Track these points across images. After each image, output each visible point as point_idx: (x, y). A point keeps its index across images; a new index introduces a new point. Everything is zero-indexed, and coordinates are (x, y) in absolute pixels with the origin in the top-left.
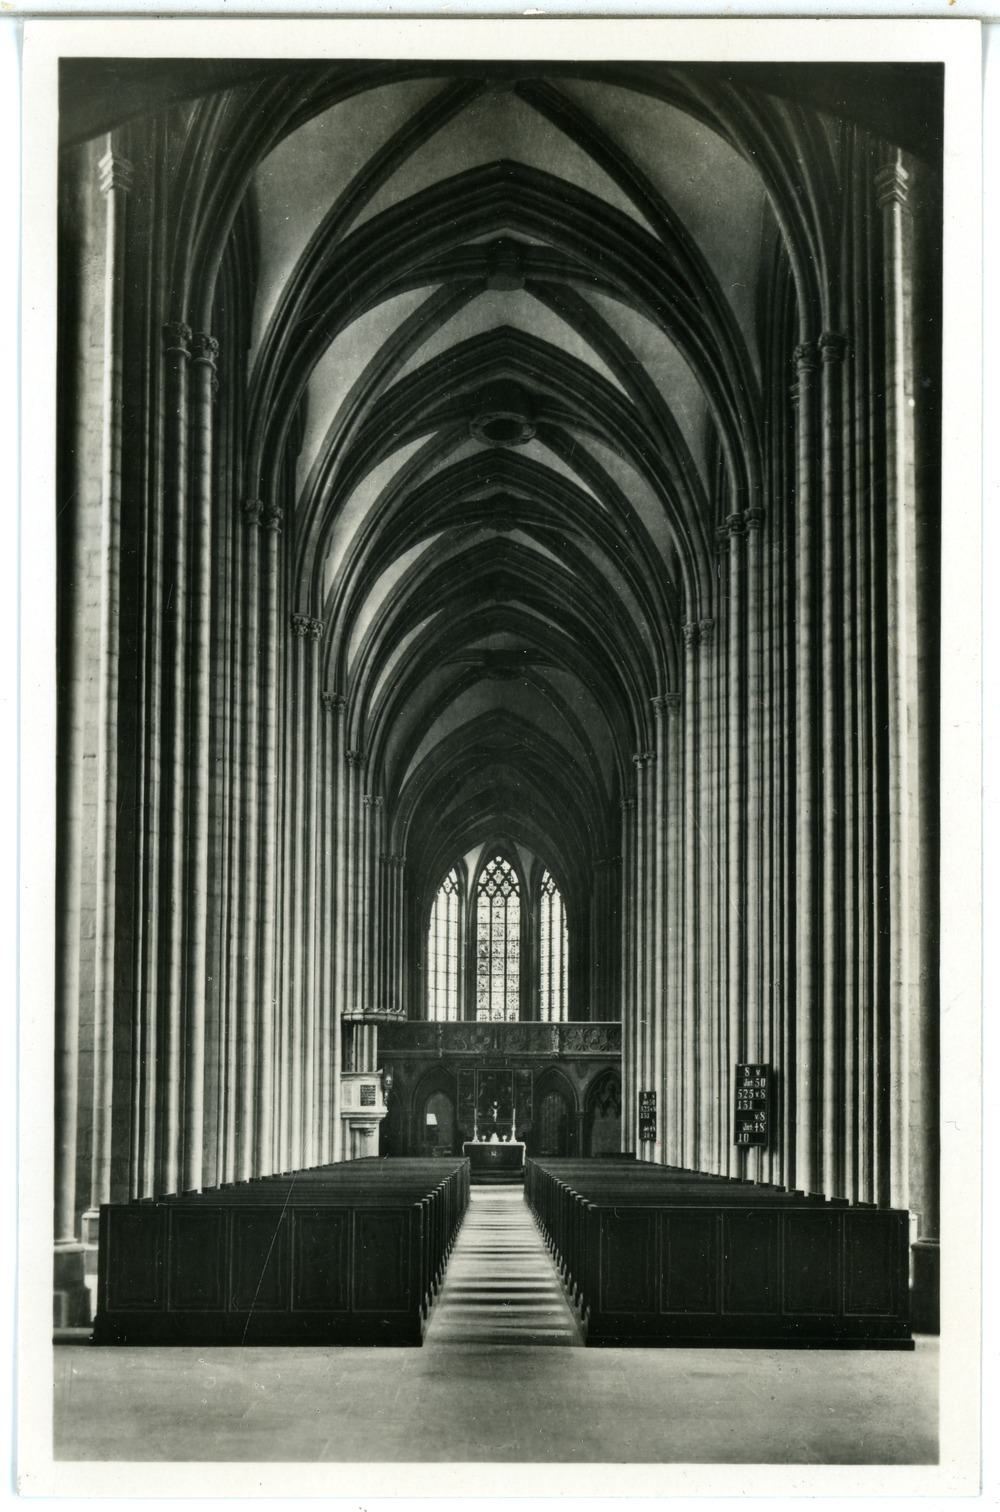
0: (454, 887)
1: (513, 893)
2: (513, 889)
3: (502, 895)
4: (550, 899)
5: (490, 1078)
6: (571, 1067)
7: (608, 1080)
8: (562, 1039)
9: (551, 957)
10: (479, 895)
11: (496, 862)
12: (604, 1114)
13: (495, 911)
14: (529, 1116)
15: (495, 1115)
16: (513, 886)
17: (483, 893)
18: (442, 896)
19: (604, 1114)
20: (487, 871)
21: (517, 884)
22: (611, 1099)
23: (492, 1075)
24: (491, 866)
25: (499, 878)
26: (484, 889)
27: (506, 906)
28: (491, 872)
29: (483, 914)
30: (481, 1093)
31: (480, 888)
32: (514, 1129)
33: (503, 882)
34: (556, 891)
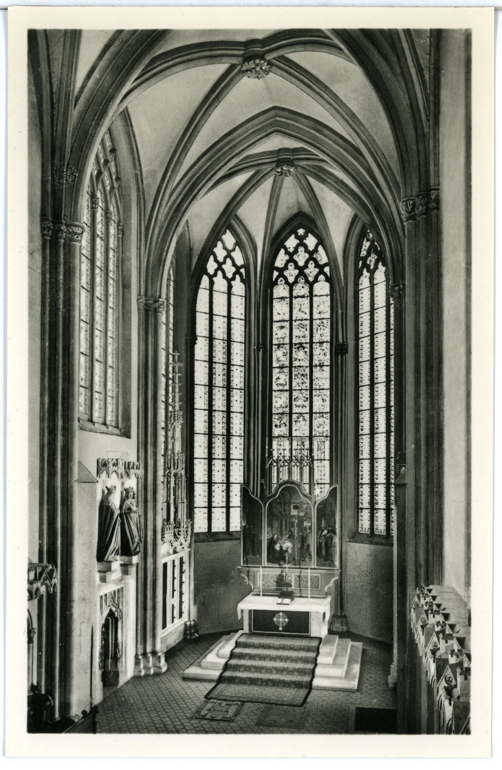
0: (238, 272)
1: (322, 277)
2: (321, 272)
3: (307, 281)
4: (372, 279)
9: (372, 360)
10: (276, 283)
11: (297, 237)
16: (321, 268)
18: (220, 284)
20: (286, 249)
21: (326, 265)
24: (291, 243)
25: (301, 258)
26: (281, 275)
27: (311, 295)
28: (291, 250)
29: (280, 310)
31: (276, 274)
34: (380, 265)
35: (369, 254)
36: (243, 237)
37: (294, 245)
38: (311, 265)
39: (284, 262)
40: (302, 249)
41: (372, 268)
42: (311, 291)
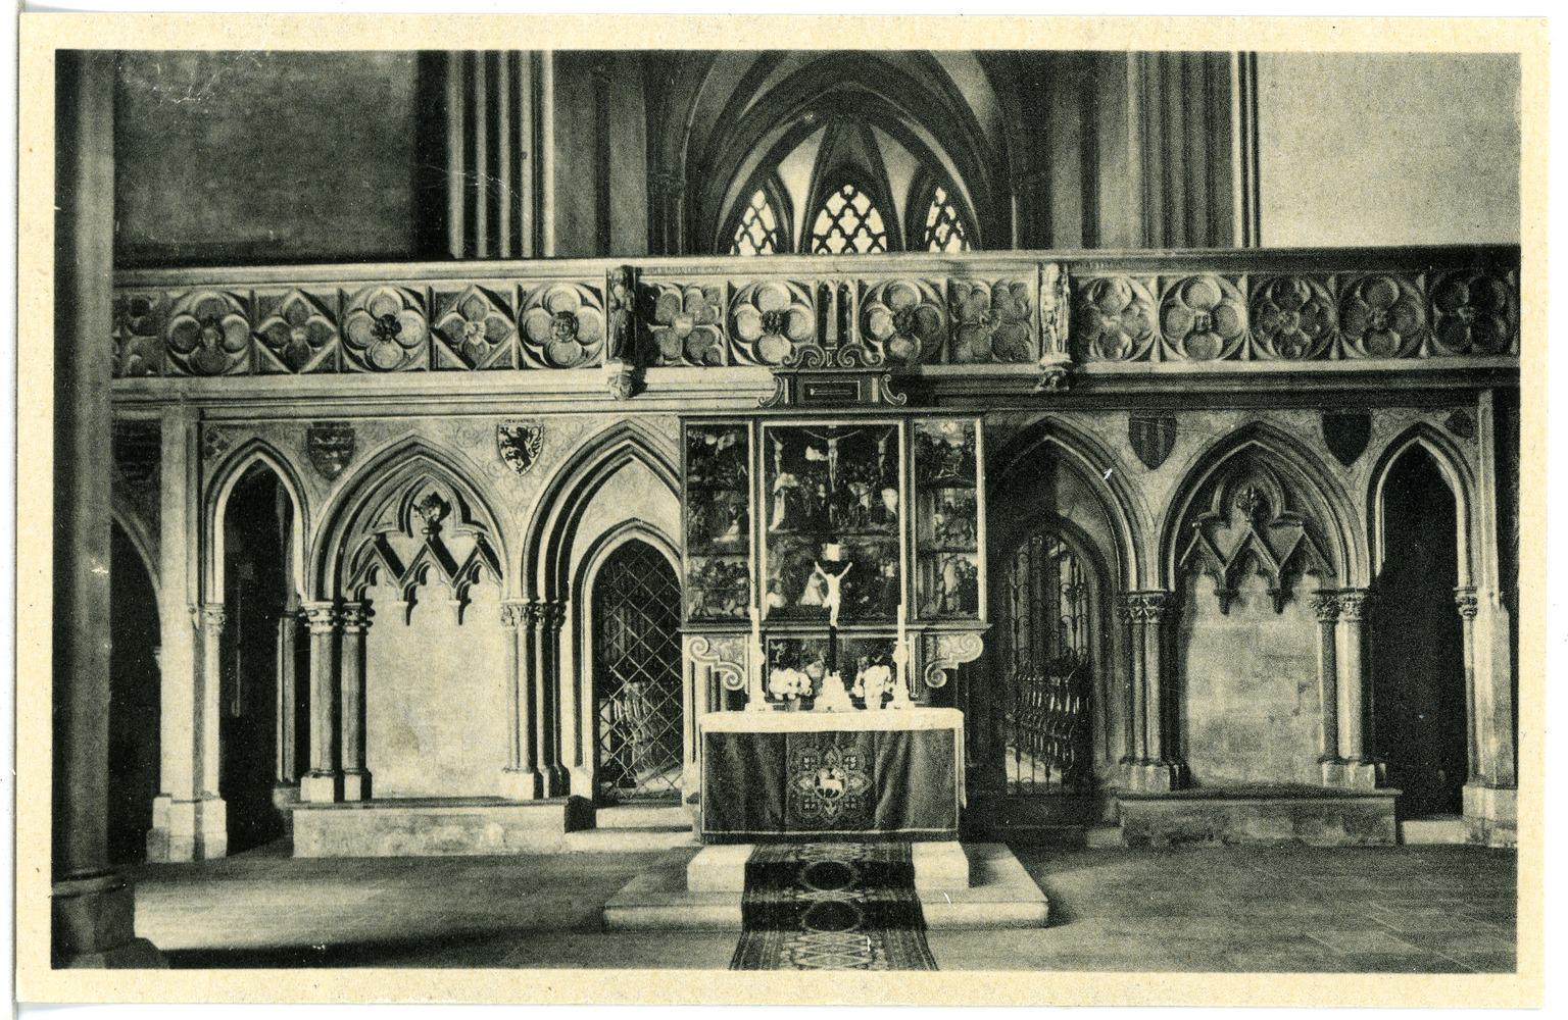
0: (768, 238)
5: (812, 454)
6: (1114, 430)
11: (844, 196)
12: (1229, 596)
14: (970, 605)
15: (833, 600)
16: (875, 238)
19: (1229, 596)
20: (829, 212)
21: (880, 235)
22: (1257, 545)
23: (824, 450)
24: (836, 203)
25: (849, 223)
26: (823, 245)
28: (835, 213)
30: (779, 515)
31: (816, 243)
33: (856, 230)
35: (938, 223)
36: (775, 193)
37: (840, 207)
38: (862, 231)
39: (827, 228)
40: (849, 212)
41: (942, 240)
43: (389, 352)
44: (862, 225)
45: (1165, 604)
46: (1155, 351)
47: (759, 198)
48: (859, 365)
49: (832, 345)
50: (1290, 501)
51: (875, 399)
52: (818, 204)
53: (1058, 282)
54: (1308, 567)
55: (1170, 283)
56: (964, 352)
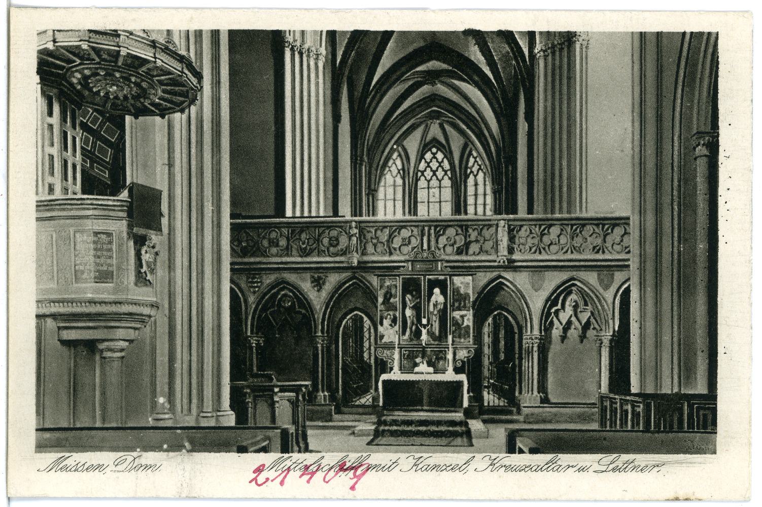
0: (399, 172)
1: (446, 177)
2: (446, 174)
3: (437, 179)
7: (570, 293)
8: (512, 239)
10: (419, 179)
11: (432, 153)
13: (431, 191)
16: (446, 172)
17: (422, 178)
20: (425, 159)
22: (573, 319)
24: (428, 156)
25: (434, 165)
26: (423, 175)
28: (428, 161)
29: (422, 195)
31: (420, 174)
32: (450, 356)
33: (437, 168)
37: (431, 158)
38: (440, 169)
42: (429, 185)
43: (274, 250)
44: (440, 166)
45: (540, 339)
46: (538, 252)
47: (395, 155)
48: (434, 257)
49: (425, 250)
50: (586, 304)
51: (439, 269)
52: (421, 157)
53: (504, 227)
54: (592, 327)
55: (543, 227)
56: (471, 251)
